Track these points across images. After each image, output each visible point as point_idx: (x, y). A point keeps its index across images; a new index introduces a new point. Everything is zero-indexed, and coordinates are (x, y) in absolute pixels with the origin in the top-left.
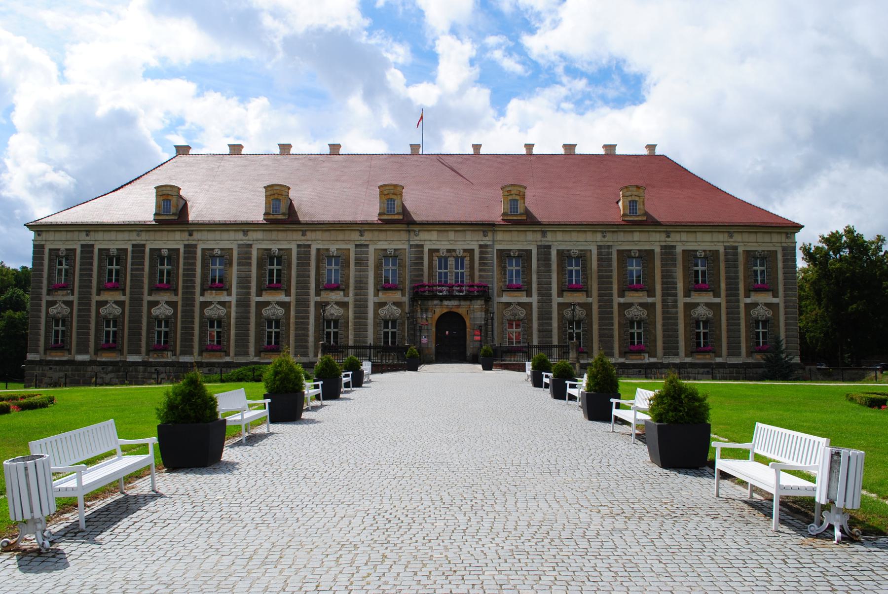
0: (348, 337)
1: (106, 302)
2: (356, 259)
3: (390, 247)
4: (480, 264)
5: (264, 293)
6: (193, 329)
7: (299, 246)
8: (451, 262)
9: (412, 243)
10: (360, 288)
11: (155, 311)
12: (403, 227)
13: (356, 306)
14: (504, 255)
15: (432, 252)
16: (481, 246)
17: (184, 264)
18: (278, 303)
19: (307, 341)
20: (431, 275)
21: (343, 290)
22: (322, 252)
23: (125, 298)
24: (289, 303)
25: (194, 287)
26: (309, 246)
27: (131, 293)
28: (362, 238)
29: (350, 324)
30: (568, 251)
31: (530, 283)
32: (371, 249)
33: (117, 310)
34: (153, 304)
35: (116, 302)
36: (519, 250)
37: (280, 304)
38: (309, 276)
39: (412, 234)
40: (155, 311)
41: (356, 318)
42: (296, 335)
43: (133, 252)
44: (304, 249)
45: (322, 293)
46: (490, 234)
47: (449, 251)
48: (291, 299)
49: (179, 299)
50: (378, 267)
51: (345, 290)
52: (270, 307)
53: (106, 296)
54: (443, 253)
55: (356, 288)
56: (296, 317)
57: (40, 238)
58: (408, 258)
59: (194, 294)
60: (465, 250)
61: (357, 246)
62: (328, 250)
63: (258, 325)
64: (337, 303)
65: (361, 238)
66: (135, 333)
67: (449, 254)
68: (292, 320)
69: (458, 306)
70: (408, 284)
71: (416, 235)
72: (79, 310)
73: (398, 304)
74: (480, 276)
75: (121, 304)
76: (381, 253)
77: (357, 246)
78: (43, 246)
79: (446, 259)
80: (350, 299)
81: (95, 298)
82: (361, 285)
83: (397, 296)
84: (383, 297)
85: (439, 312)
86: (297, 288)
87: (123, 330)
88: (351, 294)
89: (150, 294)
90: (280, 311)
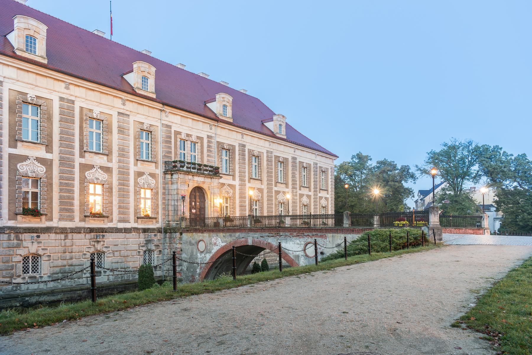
0: (112, 203)
2: (119, 127)
3: (147, 122)
4: (208, 150)
5: (19, 144)
7: (61, 99)
8: (188, 145)
9: (163, 122)
10: (123, 156)
12: (160, 106)
13: (120, 173)
14: (221, 147)
15: (177, 133)
16: (208, 137)
18: (38, 159)
19: (72, 205)
20: (176, 154)
21: (107, 155)
22: (85, 112)
24: (52, 161)
26: (73, 102)
28: (125, 107)
29: (114, 190)
30: (253, 151)
31: (234, 171)
32: (132, 119)
36: (229, 145)
37: (40, 160)
38: (73, 135)
39: (163, 113)
41: (120, 184)
42: (61, 197)
44: (67, 104)
45: (87, 155)
46: (213, 127)
47: (188, 135)
48: (55, 156)
50: (138, 138)
51: (109, 155)
52: (28, 162)
54: (183, 136)
55: (120, 155)
56: (61, 178)
58: (160, 134)
60: (198, 137)
61: (119, 113)
62: (91, 111)
63: (12, 182)
64: (101, 168)
65: (122, 107)
68: (56, 181)
69: (204, 182)
70: (160, 160)
71: (167, 116)
73: (152, 175)
74: (208, 161)
76: (140, 126)
77: (119, 113)
79: (184, 141)
80: (114, 165)
82: (123, 153)
83: (150, 168)
84: (141, 167)
86: (61, 146)
88: (114, 161)
90: (41, 170)
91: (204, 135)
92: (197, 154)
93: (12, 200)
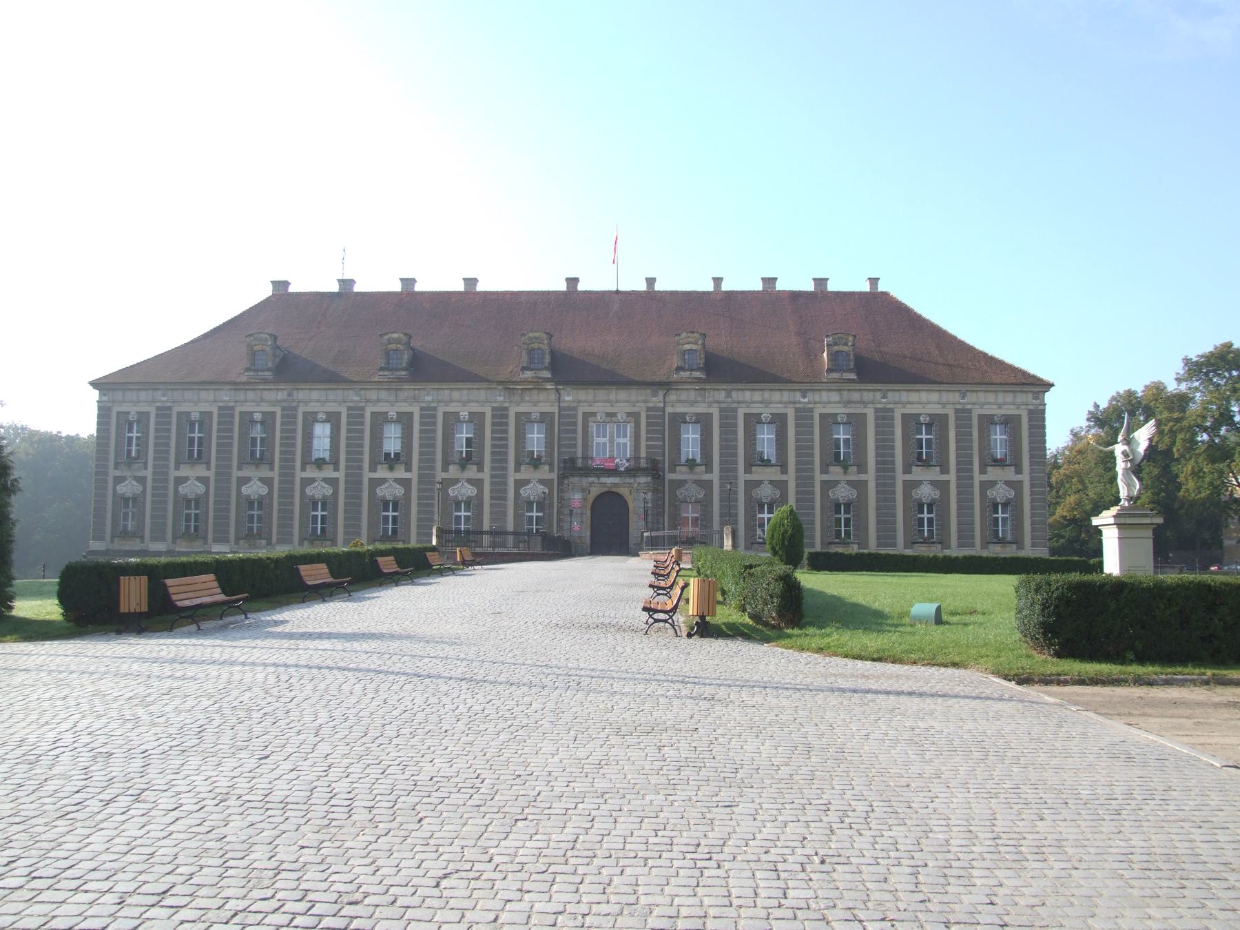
1: (186, 479)
3: (535, 411)
6: (292, 511)
11: (246, 490)
15: (587, 416)
17: (282, 431)
23: (211, 474)
25: (293, 460)
27: (217, 466)
33: (201, 489)
34: (243, 481)
35: (198, 479)
36: (697, 414)
40: (246, 490)
43: (219, 416)
47: (609, 415)
49: (275, 474)
52: (387, 485)
53: (185, 471)
57: (105, 398)
59: (293, 468)
60: (629, 414)
66: (222, 517)
67: (608, 419)
72: (154, 488)
74: (648, 447)
75: (204, 480)
78: (109, 409)
81: (173, 474)
85: (595, 491)
87: (207, 512)
89: (239, 469)
91: (641, 408)
92: (627, 441)
93: (371, 525)
